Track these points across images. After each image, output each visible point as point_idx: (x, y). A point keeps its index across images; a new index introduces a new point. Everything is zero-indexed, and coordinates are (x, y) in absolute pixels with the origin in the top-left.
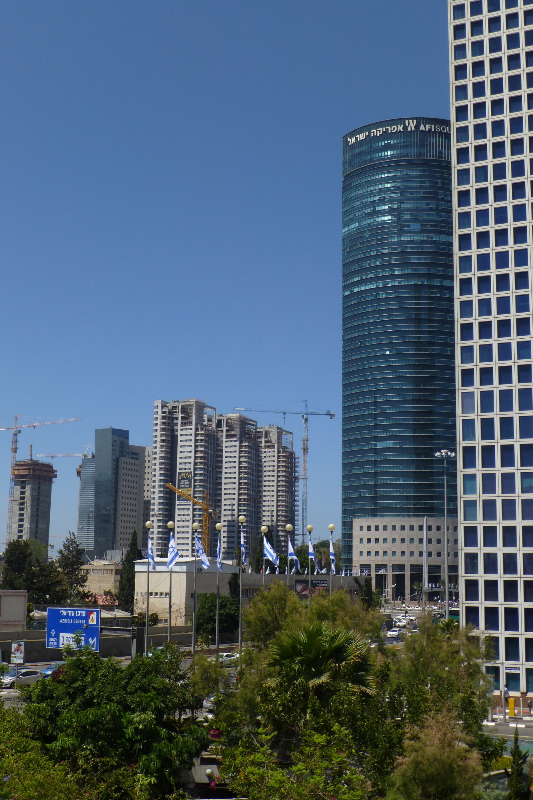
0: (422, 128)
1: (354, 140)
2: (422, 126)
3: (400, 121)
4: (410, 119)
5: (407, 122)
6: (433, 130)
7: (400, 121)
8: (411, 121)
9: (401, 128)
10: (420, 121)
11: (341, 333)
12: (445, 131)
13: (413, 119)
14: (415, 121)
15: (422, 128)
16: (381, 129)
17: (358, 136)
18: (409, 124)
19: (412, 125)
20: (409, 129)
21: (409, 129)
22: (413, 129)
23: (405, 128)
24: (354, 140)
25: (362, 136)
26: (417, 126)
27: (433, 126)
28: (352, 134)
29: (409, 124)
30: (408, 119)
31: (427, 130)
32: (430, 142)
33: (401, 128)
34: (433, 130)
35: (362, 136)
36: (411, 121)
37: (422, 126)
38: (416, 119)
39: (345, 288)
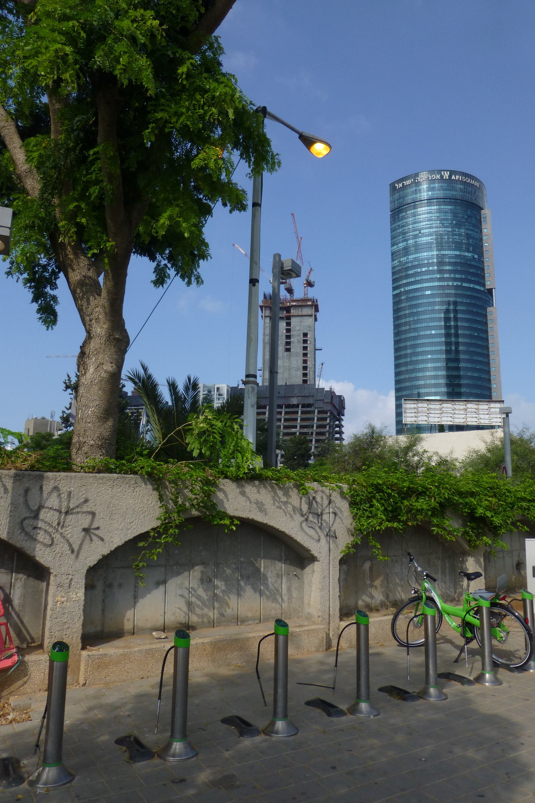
2: (453, 176)
3: (439, 172)
4: (445, 170)
5: (443, 173)
7: (439, 172)
8: (445, 172)
9: (438, 177)
10: (452, 173)
11: (392, 320)
13: (447, 171)
14: (448, 173)
15: (453, 177)
19: (446, 175)
20: (445, 178)
22: (447, 178)
23: (442, 176)
24: (401, 185)
26: (450, 176)
28: (399, 181)
30: (444, 171)
33: (438, 177)
37: (453, 176)
38: (449, 171)
39: (394, 289)
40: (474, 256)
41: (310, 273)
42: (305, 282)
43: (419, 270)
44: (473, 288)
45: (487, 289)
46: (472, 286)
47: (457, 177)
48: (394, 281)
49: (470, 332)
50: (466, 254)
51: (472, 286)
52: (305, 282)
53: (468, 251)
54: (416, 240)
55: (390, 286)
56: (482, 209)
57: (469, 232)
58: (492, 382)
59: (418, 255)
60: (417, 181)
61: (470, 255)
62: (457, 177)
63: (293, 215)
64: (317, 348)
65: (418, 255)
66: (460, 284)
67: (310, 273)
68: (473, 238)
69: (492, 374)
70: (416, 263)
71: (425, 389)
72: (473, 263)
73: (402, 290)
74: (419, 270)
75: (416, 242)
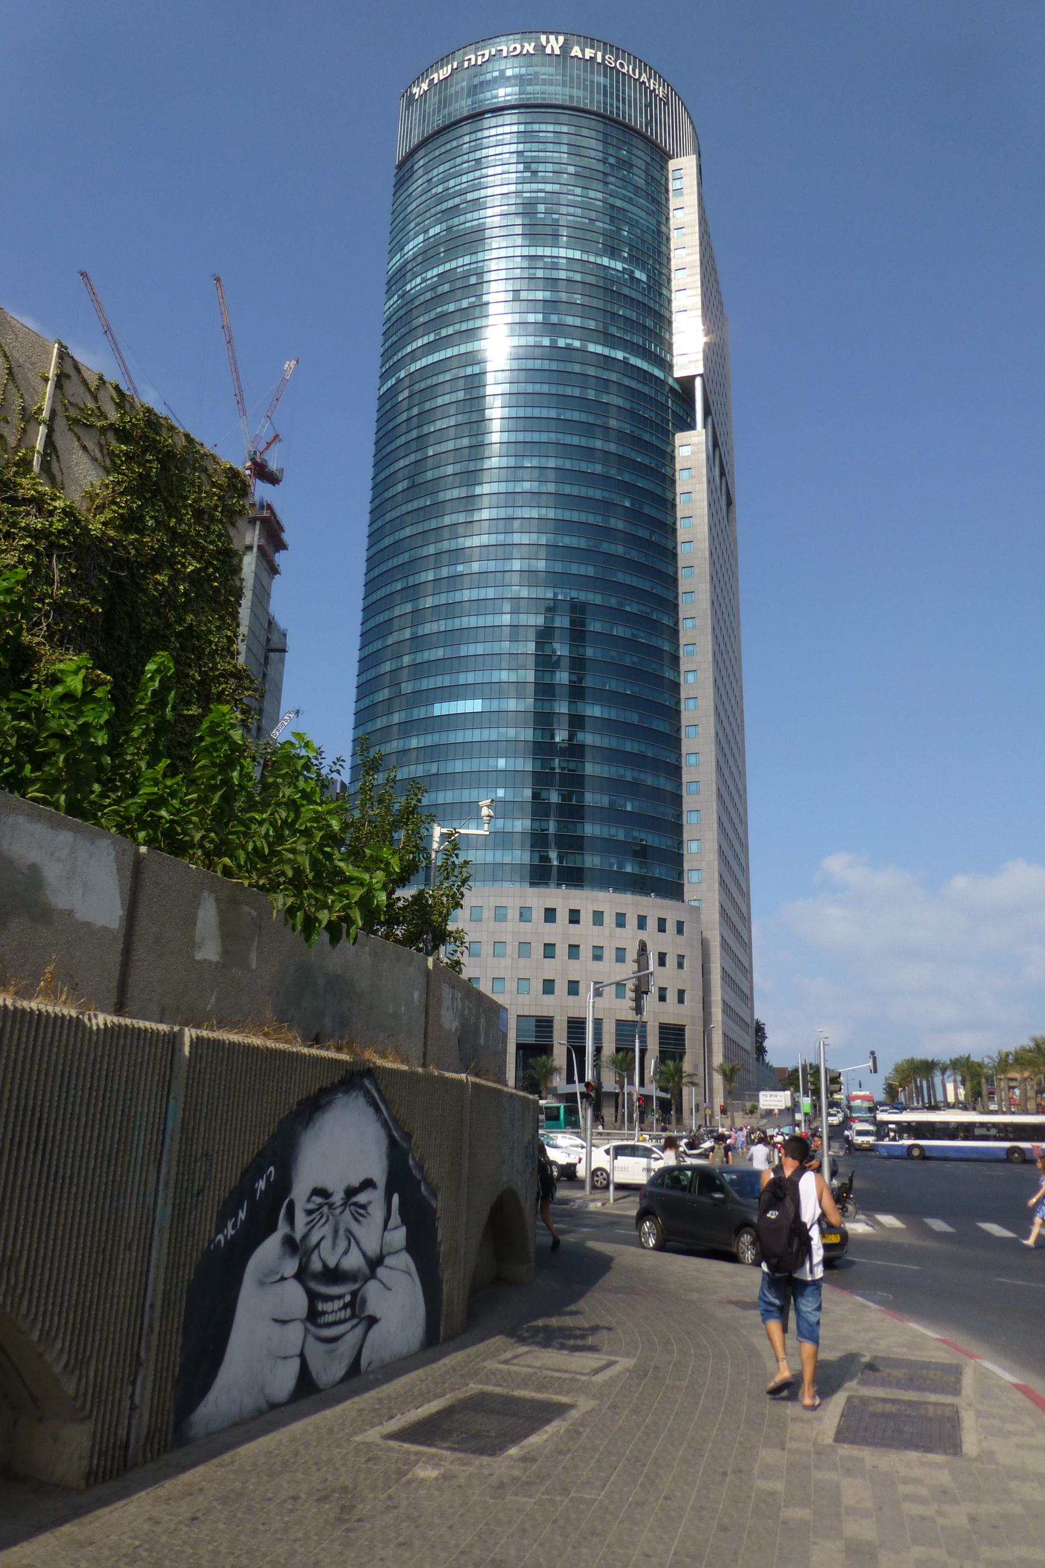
0: (576, 51)
1: (425, 86)
4: (552, 33)
5: (543, 38)
6: (599, 60)
9: (529, 48)
12: (625, 71)
14: (561, 39)
15: (576, 51)
16: (487, 52)
17: (435, 76)
18: (548, 42)
20: (548, 51)
21: (548, 51)
22: (557, 52)
24: (425, 86)
25: (444, 72)
26: (565, 48)
27: (599, 55)
29: (548, 42)
31: (587, 57)
32: (592, 82)
34: (599, 60)
35: (444, 72)
36: (552, 38)
39: (384, 377)
40: (632, 272)
41: (269, 444)
42: (249, 464)
43: (452, 307)
44: (625, 363)
45: (678, 380)
46: (620, 355)
47: (589, 53)
48: (387, 355)
49: (606, 494)
50: (605, 261)
51: (620, 355)
52: (249, 464)
53: (613, 253)
54: (450, 223)
55: (375, 367)
56: (671, 157)
57: (619, 203)
58: (683, 667)
59: (454, 264)
60: (466, 64)
61: (619, 266)
62: (589, 53)
63: (218, 280)
64: (273, 646)
65: (454, 264)
66: (577, 344)
67: (269, 444)
68: (632, 224)
69: (683, 640)
70: (446, 288)
71: (439, 678)
72: (626, 291)
73: (402, 374)
74: (452, 307)
75: (449, 229)
